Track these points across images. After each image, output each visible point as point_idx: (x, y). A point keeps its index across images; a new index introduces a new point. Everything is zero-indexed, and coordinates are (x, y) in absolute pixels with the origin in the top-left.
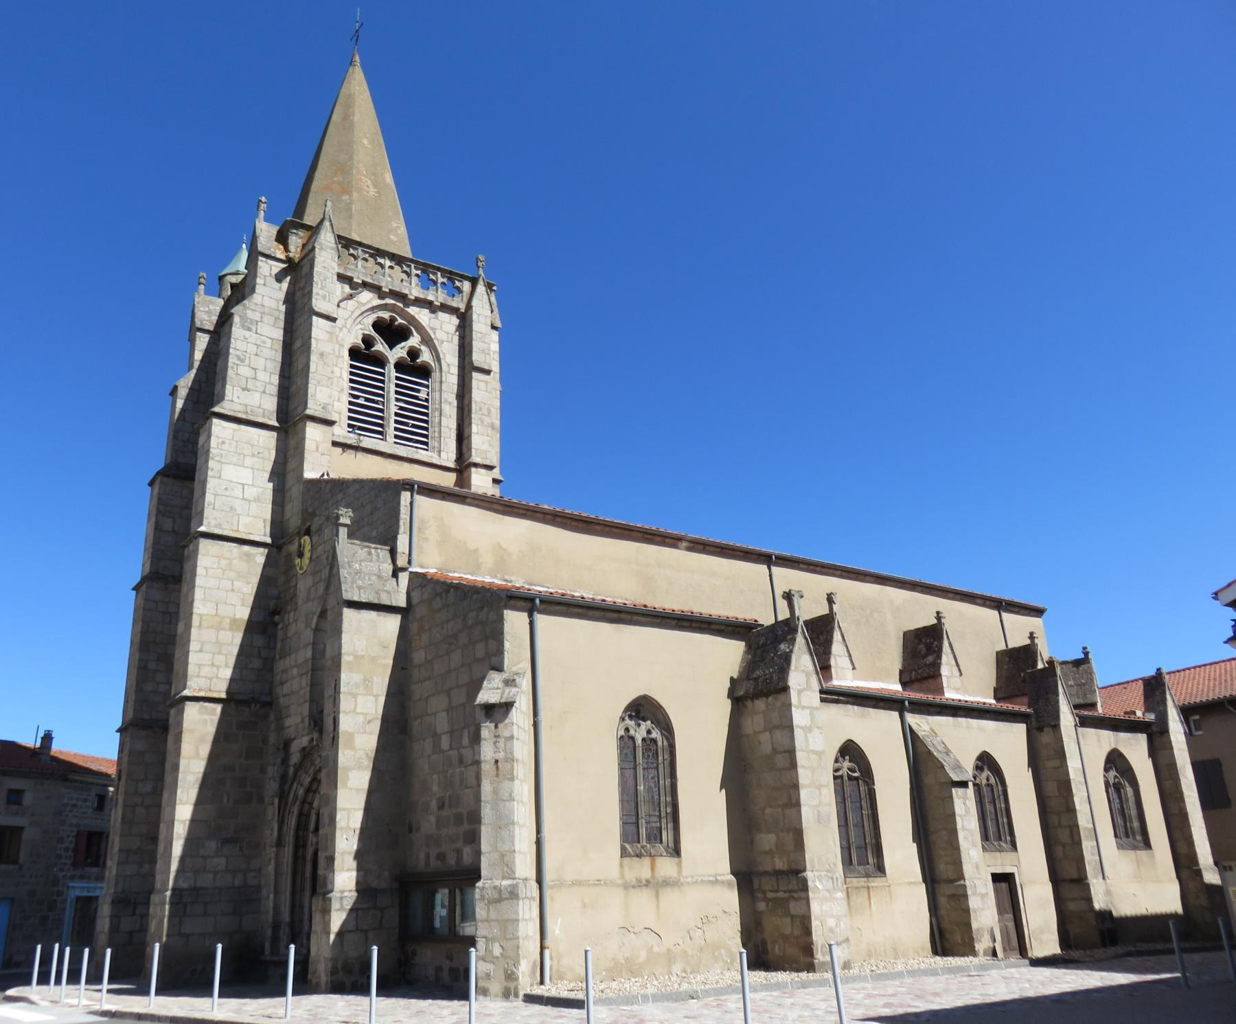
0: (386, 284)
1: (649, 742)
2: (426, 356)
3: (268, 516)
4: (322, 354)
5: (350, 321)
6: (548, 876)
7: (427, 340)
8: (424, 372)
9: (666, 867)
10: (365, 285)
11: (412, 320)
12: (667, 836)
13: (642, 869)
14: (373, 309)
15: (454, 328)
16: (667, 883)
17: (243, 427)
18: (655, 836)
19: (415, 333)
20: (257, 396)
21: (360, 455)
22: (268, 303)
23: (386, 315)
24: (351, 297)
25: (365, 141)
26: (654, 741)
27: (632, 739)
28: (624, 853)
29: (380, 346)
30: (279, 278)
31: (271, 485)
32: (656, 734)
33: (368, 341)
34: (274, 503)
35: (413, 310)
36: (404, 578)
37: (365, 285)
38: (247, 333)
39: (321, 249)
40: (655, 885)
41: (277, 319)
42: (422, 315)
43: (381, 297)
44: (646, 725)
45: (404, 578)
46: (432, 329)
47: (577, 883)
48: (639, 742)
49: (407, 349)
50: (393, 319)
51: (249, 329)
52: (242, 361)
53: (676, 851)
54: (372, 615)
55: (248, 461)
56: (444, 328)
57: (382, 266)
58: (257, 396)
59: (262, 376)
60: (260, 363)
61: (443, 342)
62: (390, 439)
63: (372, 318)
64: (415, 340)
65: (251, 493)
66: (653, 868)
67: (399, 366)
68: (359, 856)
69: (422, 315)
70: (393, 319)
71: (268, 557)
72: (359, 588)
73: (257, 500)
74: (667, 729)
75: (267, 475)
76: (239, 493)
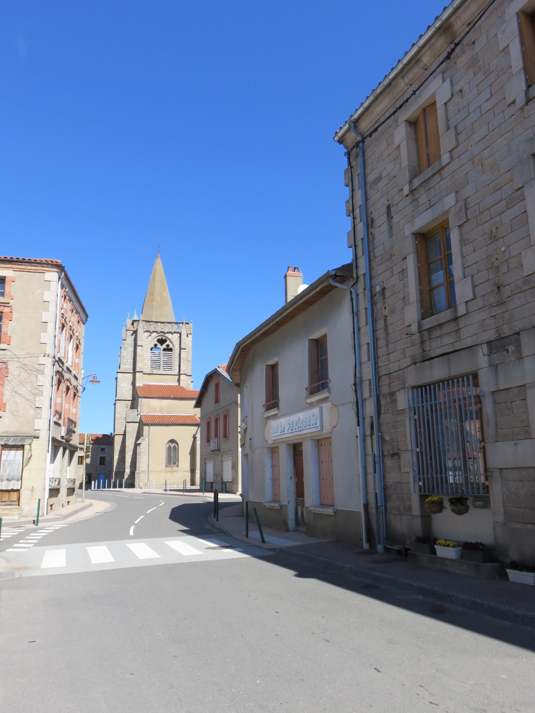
0: (159, 330)
1: (174, 447)
2: (171, 346)
3: (131, 393)
4: (140, 355)
5: (150, 342)
6: (149, 471)
7: (171, 342)
8: (171, 350)
9: (175, 468)
10: (153, 332)
11: (167, 337)
12: (177, 463)
13: (170, 469)
14: (156, 337)
15: (178, 337)
16: (174, 471)
17: (125, 374)
18: (174, 463)
19: (168, 340)
20: (128, 366)
21: (153, 375)
22: (130, 342)
23: (160, 338)
24: (150, 335)
25: (159, 284)
26: (176, 447)
27: (171, 447)
28: (166, 466)
29: (159, 345)
30: (132, 335)
31: (132, 386)
32: (176, 445)
33: (156, 345)
34: (132, 390)
35: (167, 335)
36: (139, 416)
37: (153, 332)
38: (125, 351)
39: (139, 328)
40: (172, 472)
41: (132, 346)
42: (169, 336)
43: (158, 333)
44: (174, 444)
45: (139, 416)
46: (172, 339)
47: (156, 471)
48: (172, 447)
49: (166, 345)
50: (162, 338)
51: (125, 350)
52: (124, 358)
53: (178, 466)
54: (133, 423)
55: (126, 382)
56: (174, 338)
57: (158, 325)
58: (128, 366)
59: (129, 361)
60: (128, 357)
61: (175, 342)
62: (161, 369)
63: (157, 339)
64: (168, 342)
65: (127, 389)
66: (172, 469)
67: (164, 350)
68: (130, 466)
69: (169, 336)
70: (162, 338)
71: (132, 403)
72: (130, 419)
73: (128, 390)
74: (178, 445)
75: (131, 384)
76: (124, 389)
